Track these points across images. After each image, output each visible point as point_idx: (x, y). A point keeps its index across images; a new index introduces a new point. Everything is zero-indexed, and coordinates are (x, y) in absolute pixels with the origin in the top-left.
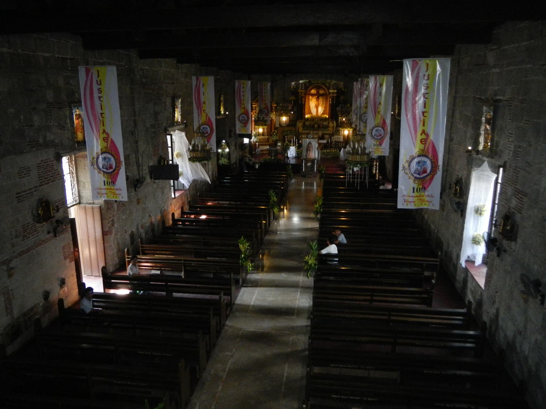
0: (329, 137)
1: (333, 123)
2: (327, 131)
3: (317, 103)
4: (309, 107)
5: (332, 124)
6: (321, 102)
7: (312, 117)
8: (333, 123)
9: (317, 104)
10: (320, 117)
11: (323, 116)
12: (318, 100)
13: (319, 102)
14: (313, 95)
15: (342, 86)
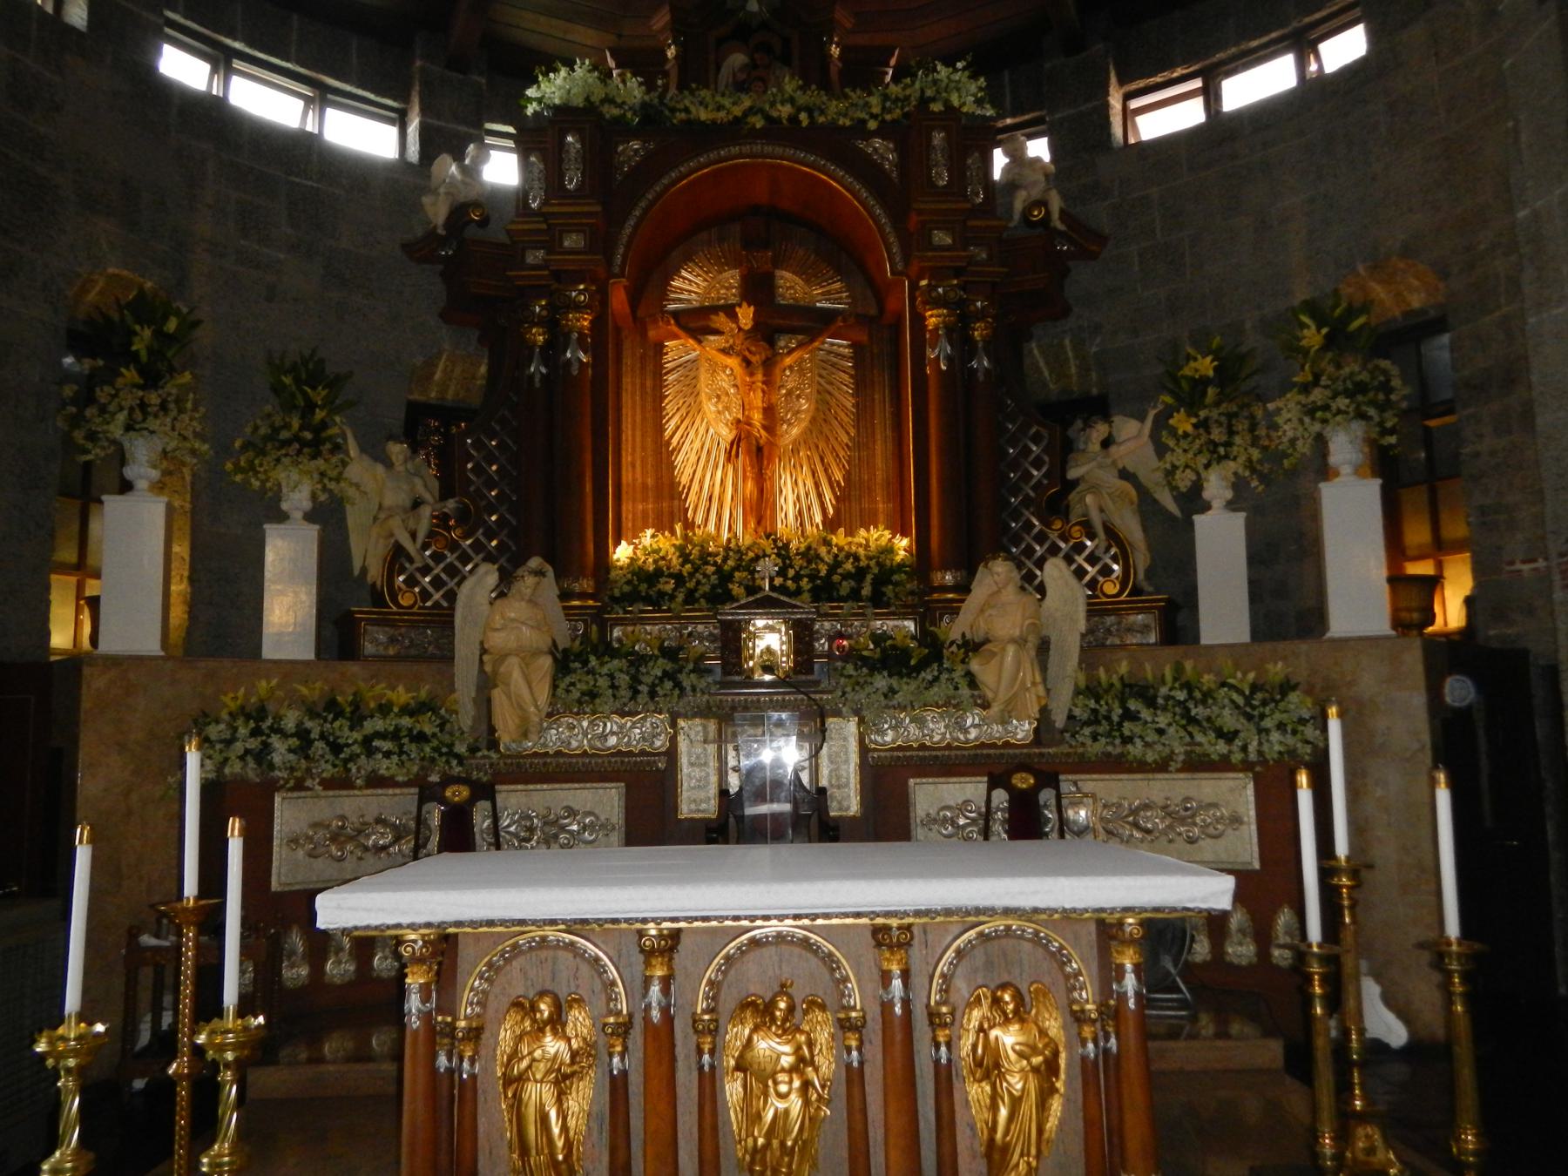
0: (1000, 797)
1: (1033, 585)
2: (951, 705)
3: (757, 399)
4: (663, 455)
5: (1010, 594)
6: (804, 404)
7: (705, 556)
8: (1033, 585)
9: (757, 417)
10: (809, 555)
11: (839, 538)
12: (769, 365)
13: (779, 397)
14: (696, 323)
15: (1056, 203)
